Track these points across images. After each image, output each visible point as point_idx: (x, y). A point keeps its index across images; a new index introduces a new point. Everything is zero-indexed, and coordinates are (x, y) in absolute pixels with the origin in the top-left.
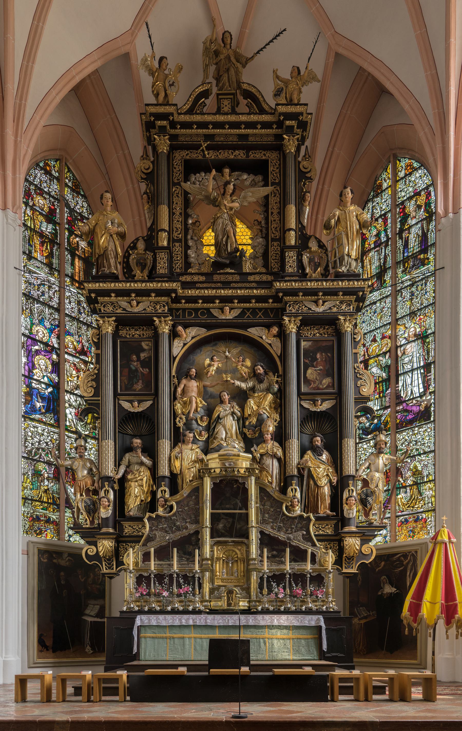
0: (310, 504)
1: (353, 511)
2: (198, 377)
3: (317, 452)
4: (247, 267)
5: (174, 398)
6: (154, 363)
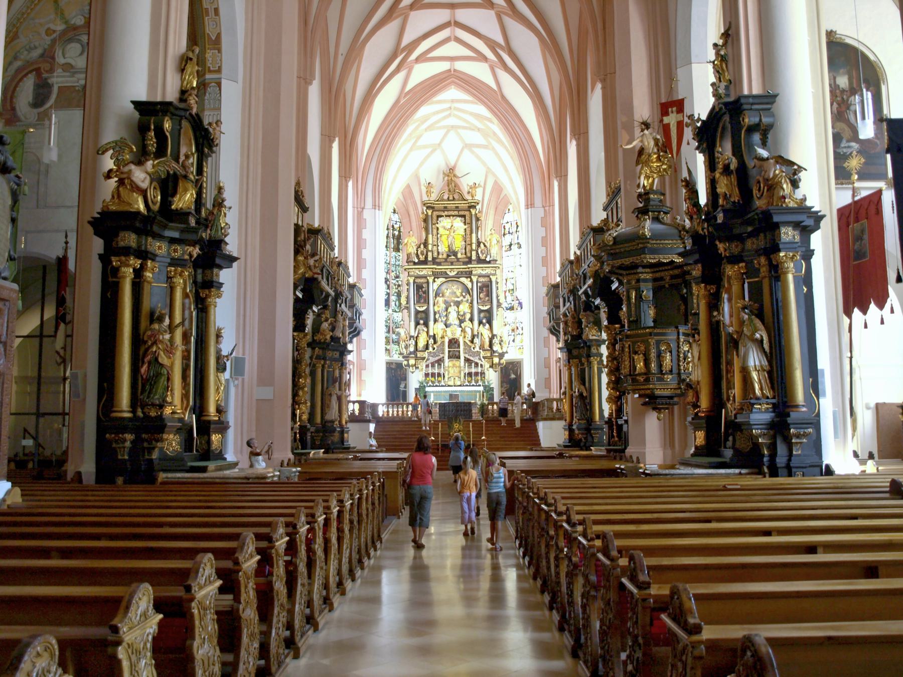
0: (482, 347)
1: (496, 347)
2: (443, 296)
3: (484, 325)
4: (459, 256)
5: (434, 305)
6: (427, 293)
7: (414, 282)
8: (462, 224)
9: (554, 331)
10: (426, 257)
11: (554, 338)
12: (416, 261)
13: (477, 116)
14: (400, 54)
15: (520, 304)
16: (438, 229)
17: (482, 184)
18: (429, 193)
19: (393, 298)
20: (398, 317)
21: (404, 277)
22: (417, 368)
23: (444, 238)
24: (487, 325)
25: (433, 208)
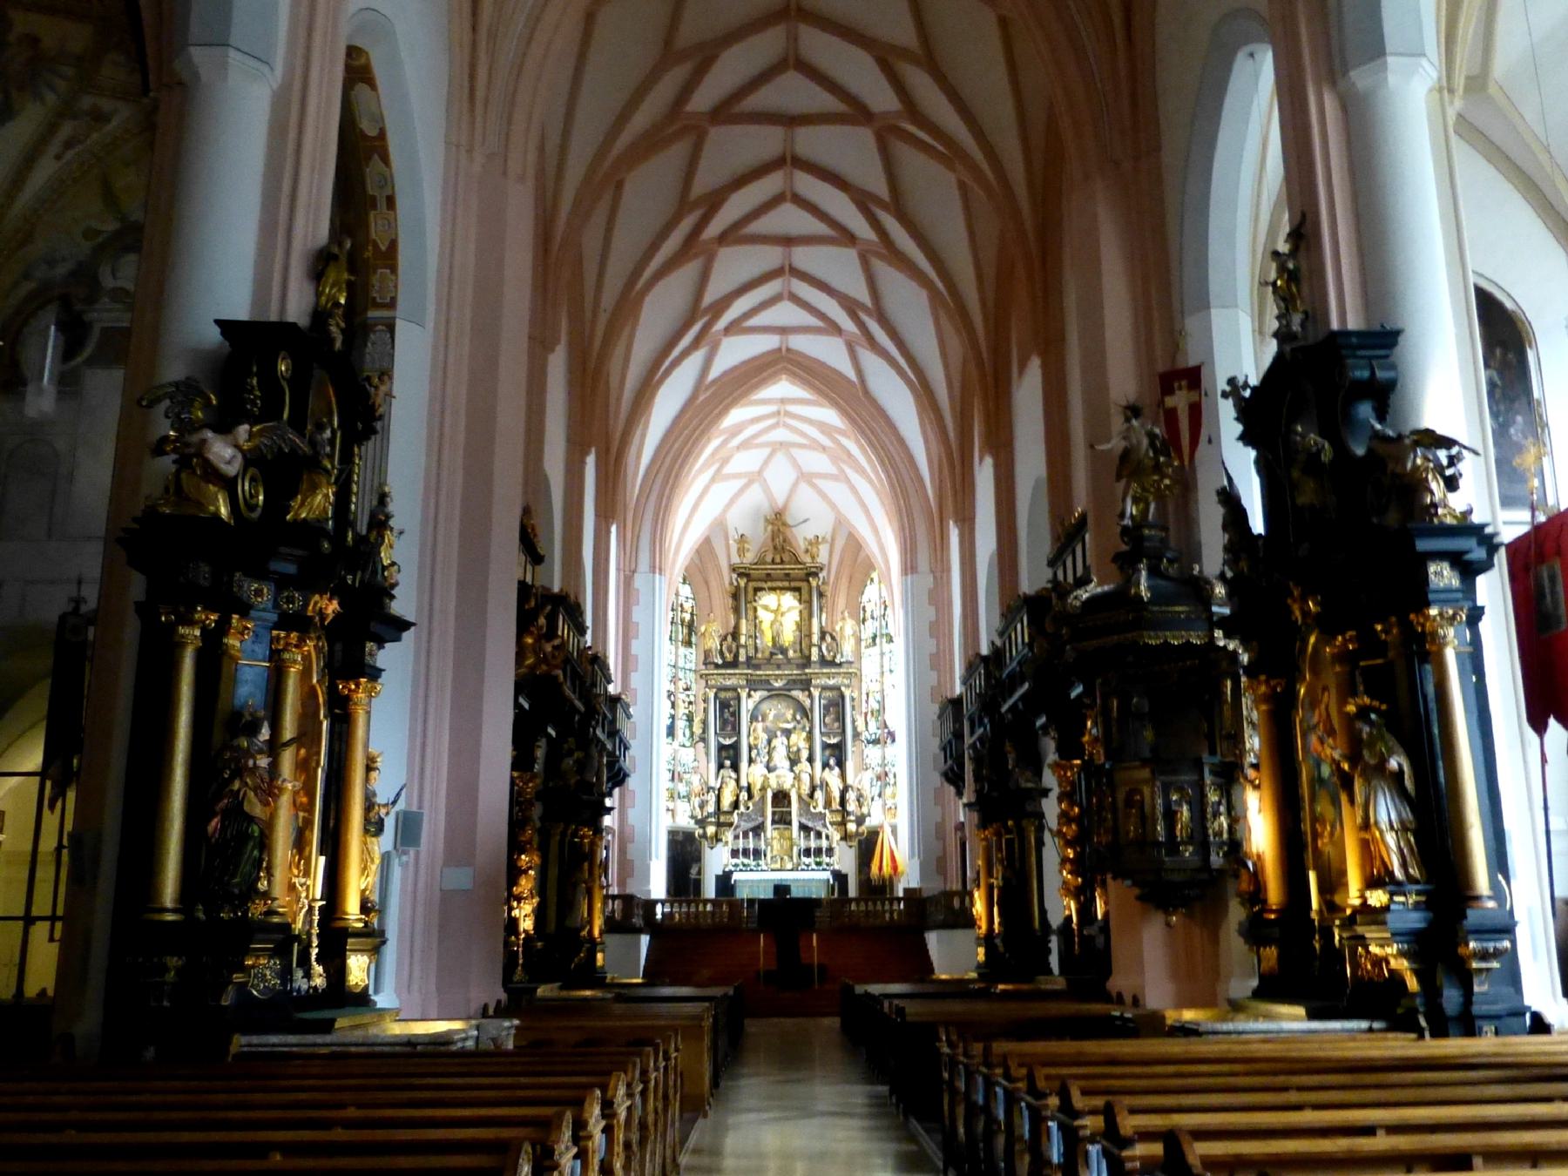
2: (763, 720)
4: (791, 653)
6: (736, 715)
7: (716, 697)
8: (796, 603)
9: (954, 777)
10: (736, 656)
11: (952, 789)
12: (720, 662)
13: (823, 427)
14: (700, 318)
15: (892, 735)
16: (755, 609)
17: (829, 538)
18: (741, 551)
19: (681, 724)
20: (687, 756)
21: (698, 688)
22: (719, 840)
23: (766, 627)
24: (837, 770)
25: (748, 576)
